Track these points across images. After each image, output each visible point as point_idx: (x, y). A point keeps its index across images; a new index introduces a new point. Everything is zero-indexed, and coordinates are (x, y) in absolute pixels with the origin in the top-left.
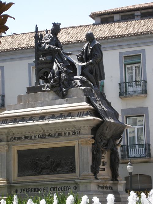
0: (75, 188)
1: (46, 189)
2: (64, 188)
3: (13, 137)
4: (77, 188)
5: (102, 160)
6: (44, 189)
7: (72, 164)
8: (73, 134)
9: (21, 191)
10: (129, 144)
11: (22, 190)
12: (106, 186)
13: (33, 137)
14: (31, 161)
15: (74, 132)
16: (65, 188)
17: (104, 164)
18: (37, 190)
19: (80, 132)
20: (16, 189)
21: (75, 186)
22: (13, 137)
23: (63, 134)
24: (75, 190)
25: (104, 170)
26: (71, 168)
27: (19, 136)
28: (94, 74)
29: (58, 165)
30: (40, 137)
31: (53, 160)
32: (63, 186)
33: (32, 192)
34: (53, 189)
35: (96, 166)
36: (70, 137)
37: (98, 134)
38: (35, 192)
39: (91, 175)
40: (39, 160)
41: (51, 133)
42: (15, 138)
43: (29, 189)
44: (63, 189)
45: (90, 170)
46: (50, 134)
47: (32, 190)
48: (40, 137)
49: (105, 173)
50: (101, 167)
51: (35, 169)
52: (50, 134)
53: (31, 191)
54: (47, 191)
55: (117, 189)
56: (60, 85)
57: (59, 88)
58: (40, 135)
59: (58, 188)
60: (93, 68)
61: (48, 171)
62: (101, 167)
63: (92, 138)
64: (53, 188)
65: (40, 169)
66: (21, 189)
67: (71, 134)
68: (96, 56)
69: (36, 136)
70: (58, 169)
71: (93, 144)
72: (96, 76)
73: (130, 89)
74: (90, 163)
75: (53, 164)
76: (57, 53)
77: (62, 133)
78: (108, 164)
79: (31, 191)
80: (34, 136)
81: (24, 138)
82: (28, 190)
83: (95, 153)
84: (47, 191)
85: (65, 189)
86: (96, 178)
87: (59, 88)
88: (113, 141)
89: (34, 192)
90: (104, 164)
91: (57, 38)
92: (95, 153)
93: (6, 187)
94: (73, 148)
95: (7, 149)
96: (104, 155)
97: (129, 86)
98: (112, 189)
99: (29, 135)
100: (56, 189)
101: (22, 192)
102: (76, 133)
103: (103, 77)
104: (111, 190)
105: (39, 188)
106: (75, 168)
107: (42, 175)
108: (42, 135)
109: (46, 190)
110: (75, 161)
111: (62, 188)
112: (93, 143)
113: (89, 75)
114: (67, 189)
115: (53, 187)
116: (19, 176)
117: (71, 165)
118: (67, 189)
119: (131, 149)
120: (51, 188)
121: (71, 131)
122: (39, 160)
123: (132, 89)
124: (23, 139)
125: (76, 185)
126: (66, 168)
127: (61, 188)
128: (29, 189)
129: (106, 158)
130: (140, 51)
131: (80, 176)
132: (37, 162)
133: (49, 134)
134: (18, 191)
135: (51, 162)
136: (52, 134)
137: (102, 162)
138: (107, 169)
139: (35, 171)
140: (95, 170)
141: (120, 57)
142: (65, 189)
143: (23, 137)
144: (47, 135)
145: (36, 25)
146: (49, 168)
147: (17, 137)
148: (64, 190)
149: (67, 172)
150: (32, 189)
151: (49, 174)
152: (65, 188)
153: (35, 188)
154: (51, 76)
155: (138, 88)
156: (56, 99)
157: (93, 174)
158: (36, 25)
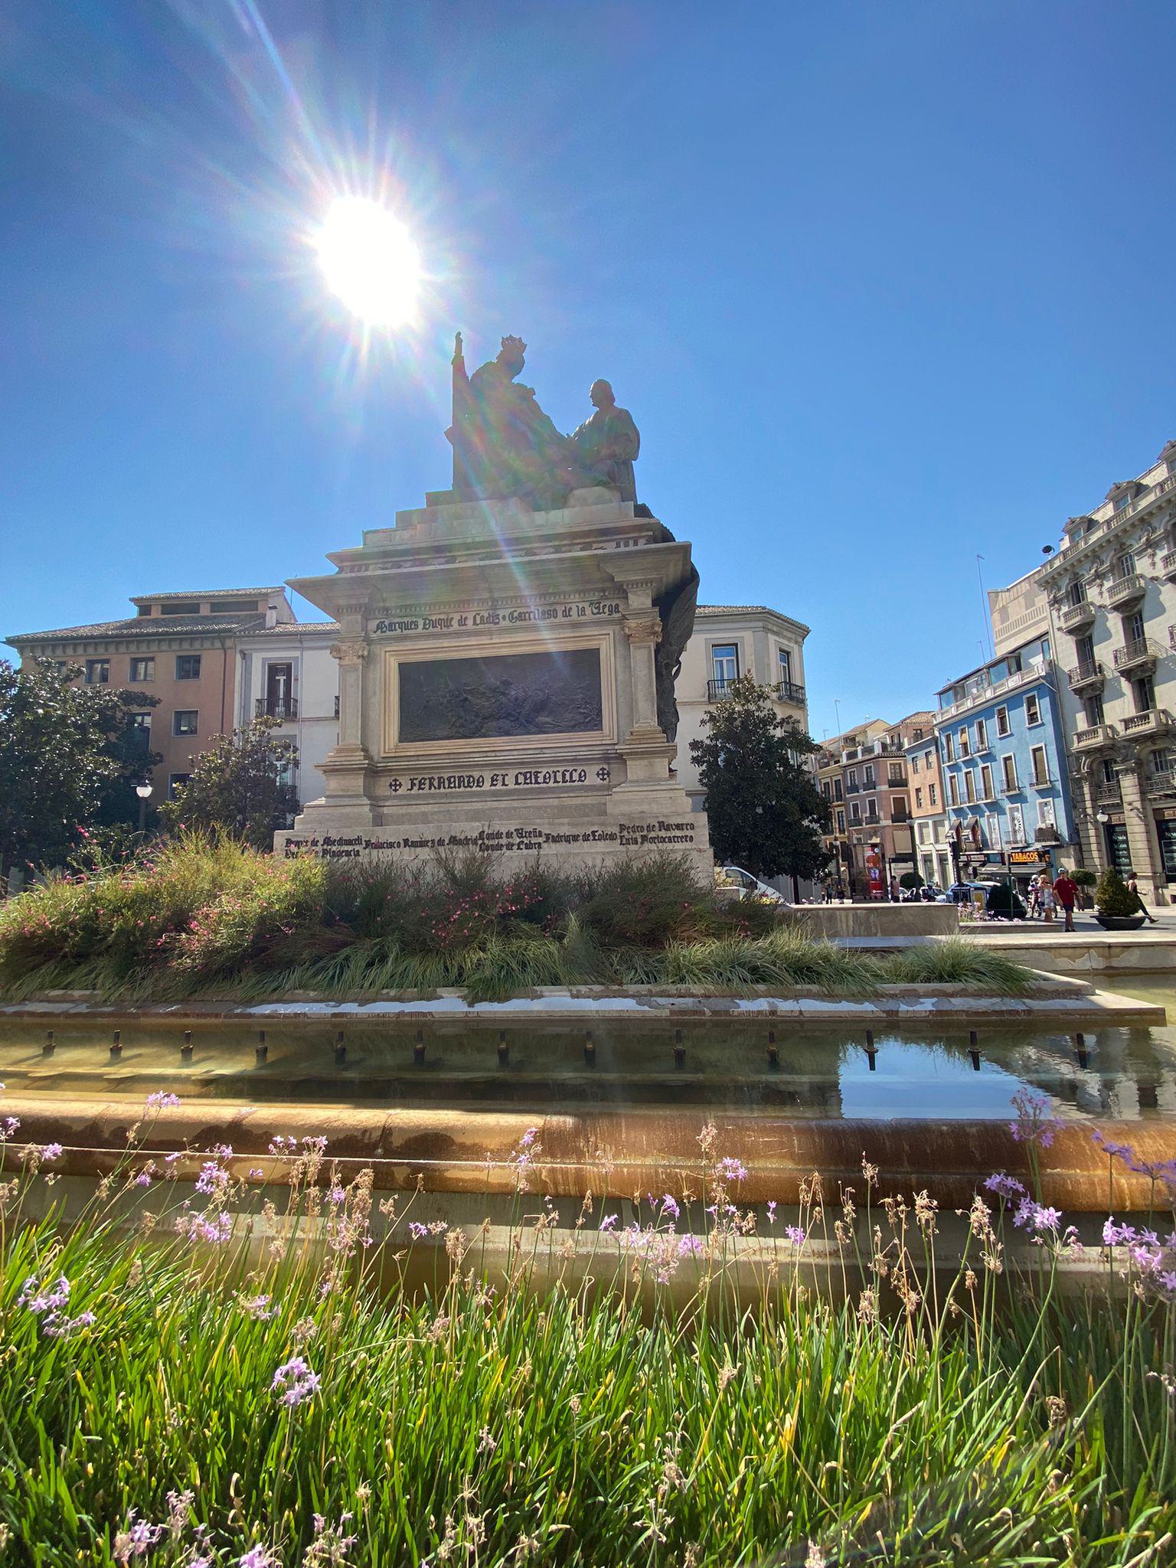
0: (603, 774)
1: (500, 778)
2: (564, 775)
3: (386, 623)
4: (608, 774)
6: (493, 780)
8: (595, 611)
9: (413, 785)
15: (599, 608)
16: (568, 774)
18: (469, 782)
20: (396, 780)
21: (603, 769)
22: (386, 623)
24: (603, 779)
26: (586, 716)
27: (405, 620)
32: (561, 769)
33: (449, 787)
34: (526, 779)
37: (673, 616)
41: (520, 610)
42: (390, 624)
43: (439, 778)
44: (559, 778)
47: (450, 783)
52: (515, 614)
53: (447, 785)
58: (478, 618)
61: (506, 724)
64: (525, 775)
67: (588, 611)
69: (466, 618)
70: (542, 719)
79: (447, 785)
81: (425, 624)
82: (436, 783)
84: (504, 784)
85: (568, 777)
89: (459, 787)
93: (360, 769)
99: (442, 617)
100: (536, 777)
102: (606, 610)
105: (476, 775)
108: (486, 615)
109: (500, 783)
111: (555, 776)
114: (576, 776)
115: (523, 771)
116: (404, 737)
118: (576, 776)
120: (517, 777)
124: (421, 626)
125: (606, 766)
127: (552, 775)
128: (439, 778)
132: (466, 699)
133: (511, 614)
134: (400, 785)
142: (568, 777)
143: (421, 622)
145: (459, 334)
148: (564, 781)
149: (573, 728)
150: (449, 779)
151: (508, 734)
152: (568, 774)
153: (459, 777)
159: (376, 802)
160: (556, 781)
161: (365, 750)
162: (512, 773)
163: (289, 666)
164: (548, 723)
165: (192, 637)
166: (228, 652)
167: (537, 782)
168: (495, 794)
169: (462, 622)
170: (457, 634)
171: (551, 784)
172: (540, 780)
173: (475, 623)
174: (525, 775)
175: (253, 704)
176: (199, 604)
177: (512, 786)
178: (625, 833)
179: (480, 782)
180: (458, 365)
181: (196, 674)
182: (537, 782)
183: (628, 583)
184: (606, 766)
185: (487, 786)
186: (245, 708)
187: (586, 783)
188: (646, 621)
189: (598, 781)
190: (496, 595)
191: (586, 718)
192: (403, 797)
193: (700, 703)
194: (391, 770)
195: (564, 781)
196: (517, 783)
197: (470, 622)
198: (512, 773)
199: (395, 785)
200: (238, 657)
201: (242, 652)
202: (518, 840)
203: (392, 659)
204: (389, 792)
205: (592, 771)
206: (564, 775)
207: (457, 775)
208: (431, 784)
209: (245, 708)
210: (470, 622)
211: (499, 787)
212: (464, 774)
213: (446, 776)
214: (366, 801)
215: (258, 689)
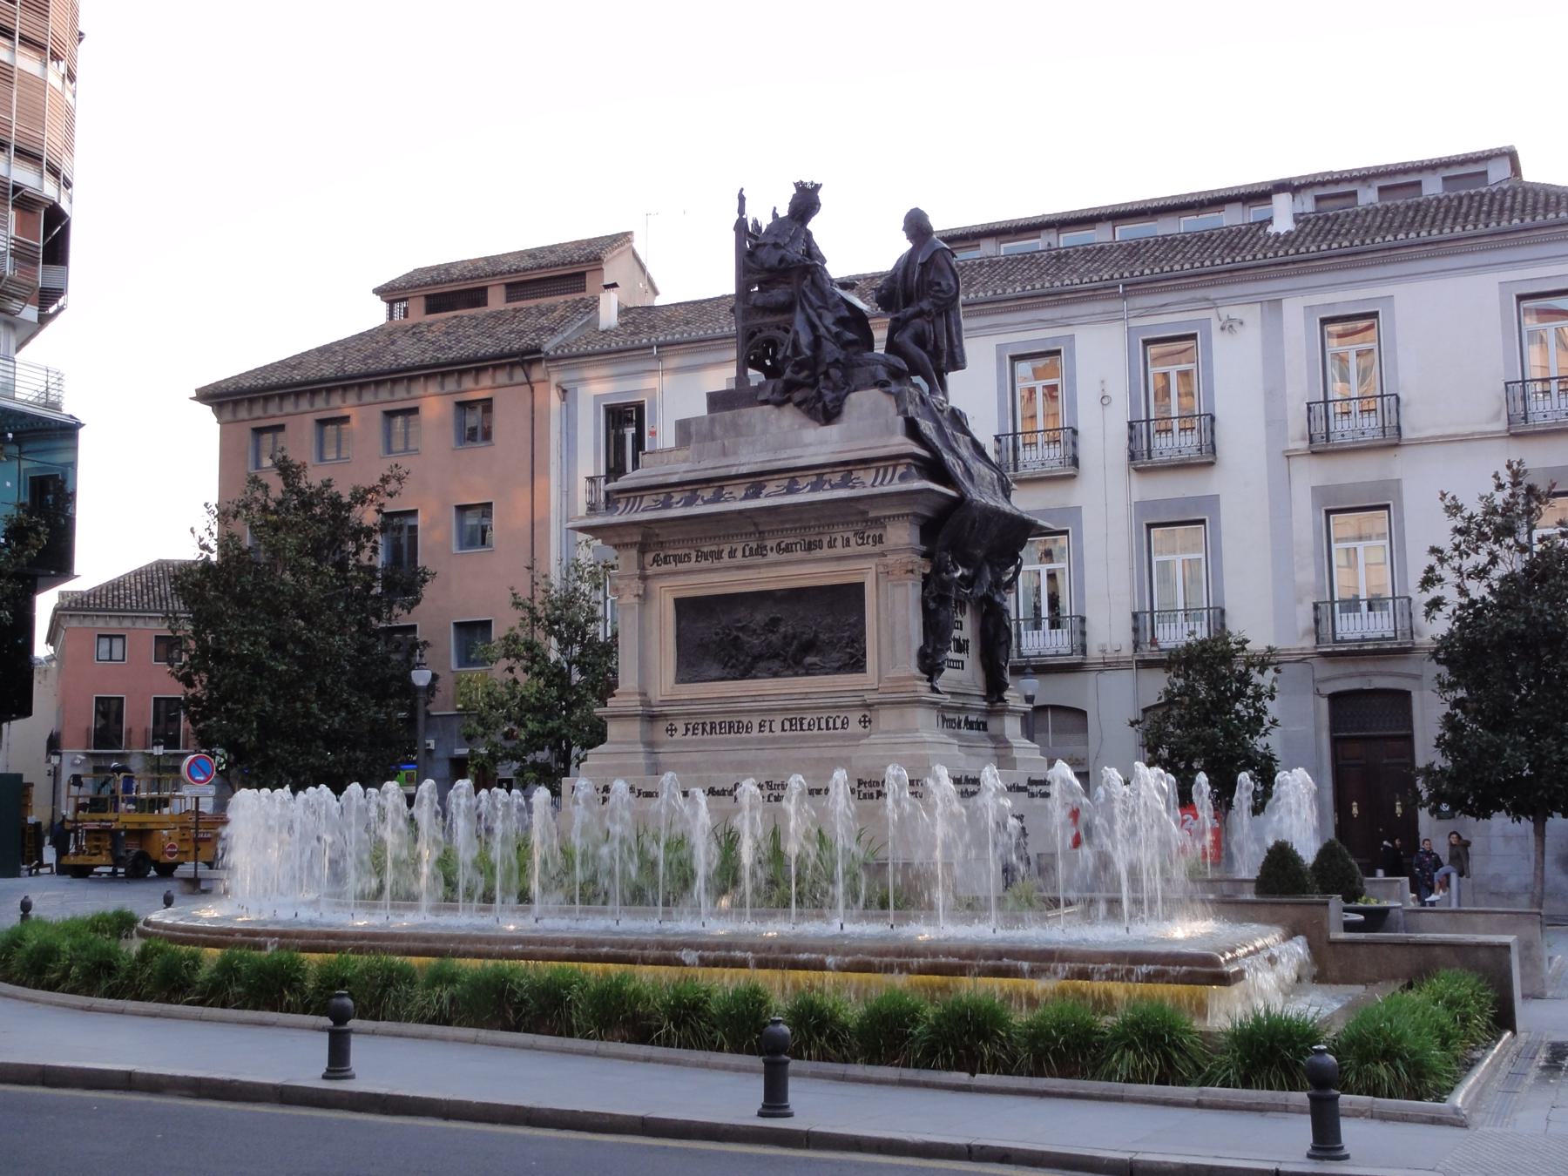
1: (767, 724)
2: (827, 722)
4: (870, 721)
5: (956, 633)
6: (761, 726)
7: (853, 641)
8: (860, 542)
9: (687, 730)
10: (1021, 617)
11: (690, 727)
12: (967, 719)
13: (725, 555)
14: (717, 634)
16: (831, 721)
17: (961, 647)
19: (881, 536)
21: (865, 716)
22: (662, 556)
23: (825, 545)
25: (960, 665)
26: (852, 656)
28: (930, 348)
29: (810, 646)
30: (747, 553)
31: (791, 631)
32: (825, 716)
35: (934, 649)
36: (848, 551)
38: (732, 734)
39: (921, 679)
40: (742, 629)
42: (665, 557)
44: (823, 725)
45: (914, 662)
46: (783, 546)
48: (747, 553)
49: (964, 673)
50: (951, 655)
51: (731, 657)
52: (783, 546)
54: (771, 731)
55: (1003, 730)
56: (817, 382)
57: (814, 393)
59: (805, 722)
60: (928, 328)
61: (776, 665)
62: (951, 655)
63: (924, 555)
64: (791, 720)
65: (749, 659)
66: (687, 725)
67: (852, 541)
68: (937, 288)
70: (809, 660)
71: (925, 576)
72: (936, 354)
73: (1028, 454)
74: (917, 641)
75: (791, 645)
76: (809, 277)
77: (820, 541)
78: (973, 649)
80: (730, 552)
82: (708, 728)
83: (932, 605)
84: (771, 731)
85: (831, 725)
86: (934, 690)
87: (814, 393)
88: (993, 572)
90: (961, 647)
91: (809, 234)
92: (932, 605)
94: (859, 588)
95: (641, 592)
96: (960, 618)
97: (1024, 445)
98: (985, 729)
100: (801, 724)
101: (690, 733)
103: (959, 359)
104: (983, 733)
105: (745, 720)
106: (864, 655)
107: (755, 677)
108: (755, 547)
109: (767, 728)
110: (863, 633)
112: (928, 571)
113: (914, 349)
114: (839, 724)
115: (790, 717)
116: (680, 680)
117: (852, 647)
118: (839, 724)
119: (1030, 632)
121: (850, 535)
122: (742, 629)
123: (1034, 453)
124: (694, 559)
126: (835, 655)
129: (966, 627)
130: (1055, 339)
131: (879, 682)
132: (737, 638)
133: (779, 545)
135: (785, 637)
136: (787, 545)
137: (955, 639)
138: (971, 660)
139: (732, 667)
140: (930, 665)
141: (1000, 359)
142: (831, 725)
143: (693, 555)
144: (772, 549)
145: (742, 190)
146: (776, 656)
147: (675, 556)
148: (828, 728)
149: (838, 670)
150: (720, 724)
151: (775, 675)
152: (831, 721)
154: (788, 353)
155: (1052, 451)
156: (802, 427)
157: (926, 676)
158: (742, 190)
159: (650, 745)
160: (819, 728)
161: (643, 694)
162: (778, 719)
163: (640, 407)
164: (816, 664)
165: (475, 366)
166: (537, 387)
167: (802, 729)
168: (760, 741)
169: (732, 554)
170: (728, 569)
171: (815, 731)
172: (805, 727)
173: (744, 556)
174: (791, 720)
175: (582, 485)
176: (484, 289)
177: (778, 733)
178: (862, 787)
179: (748, 729)
180: (741, 226)
181: (487, 435)
182: (802, 729)
183: (885, 517)
184: (867, 713)
185: (755, 733)
186: (568, 492)
187: (849, 730)
188: (905, 557)
189: (859, 729)
190: (761, 529)
191: (851, 658)
192: (677, 743)
193: (1486, 437)
194: (666, 715)
195: (828, 728)
196: (783, 730)
197: (739, 554)
198: (778, 719)
199: (671, 730)
200: (554, 397)
201: (558, 386)
202: (769, 792)
203: (668, 595)
204: (665, 737)
205: (855, 717)
206: (827, 722)
207: (727, 720)
208: (704, 729)
209: (568, 492)
210: (739, 554)
211: (767, 733)
212: (734, 720)
213: (717, 721)
214: (640, 748)
215: (590, 459)
